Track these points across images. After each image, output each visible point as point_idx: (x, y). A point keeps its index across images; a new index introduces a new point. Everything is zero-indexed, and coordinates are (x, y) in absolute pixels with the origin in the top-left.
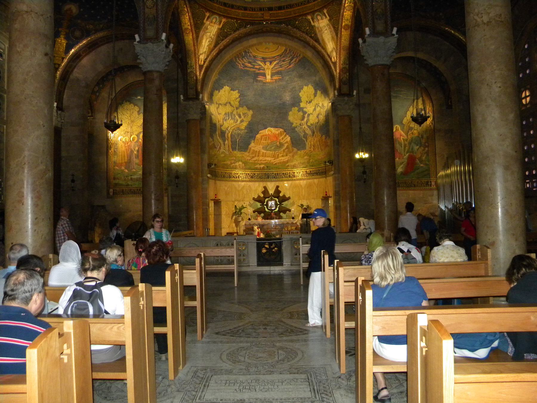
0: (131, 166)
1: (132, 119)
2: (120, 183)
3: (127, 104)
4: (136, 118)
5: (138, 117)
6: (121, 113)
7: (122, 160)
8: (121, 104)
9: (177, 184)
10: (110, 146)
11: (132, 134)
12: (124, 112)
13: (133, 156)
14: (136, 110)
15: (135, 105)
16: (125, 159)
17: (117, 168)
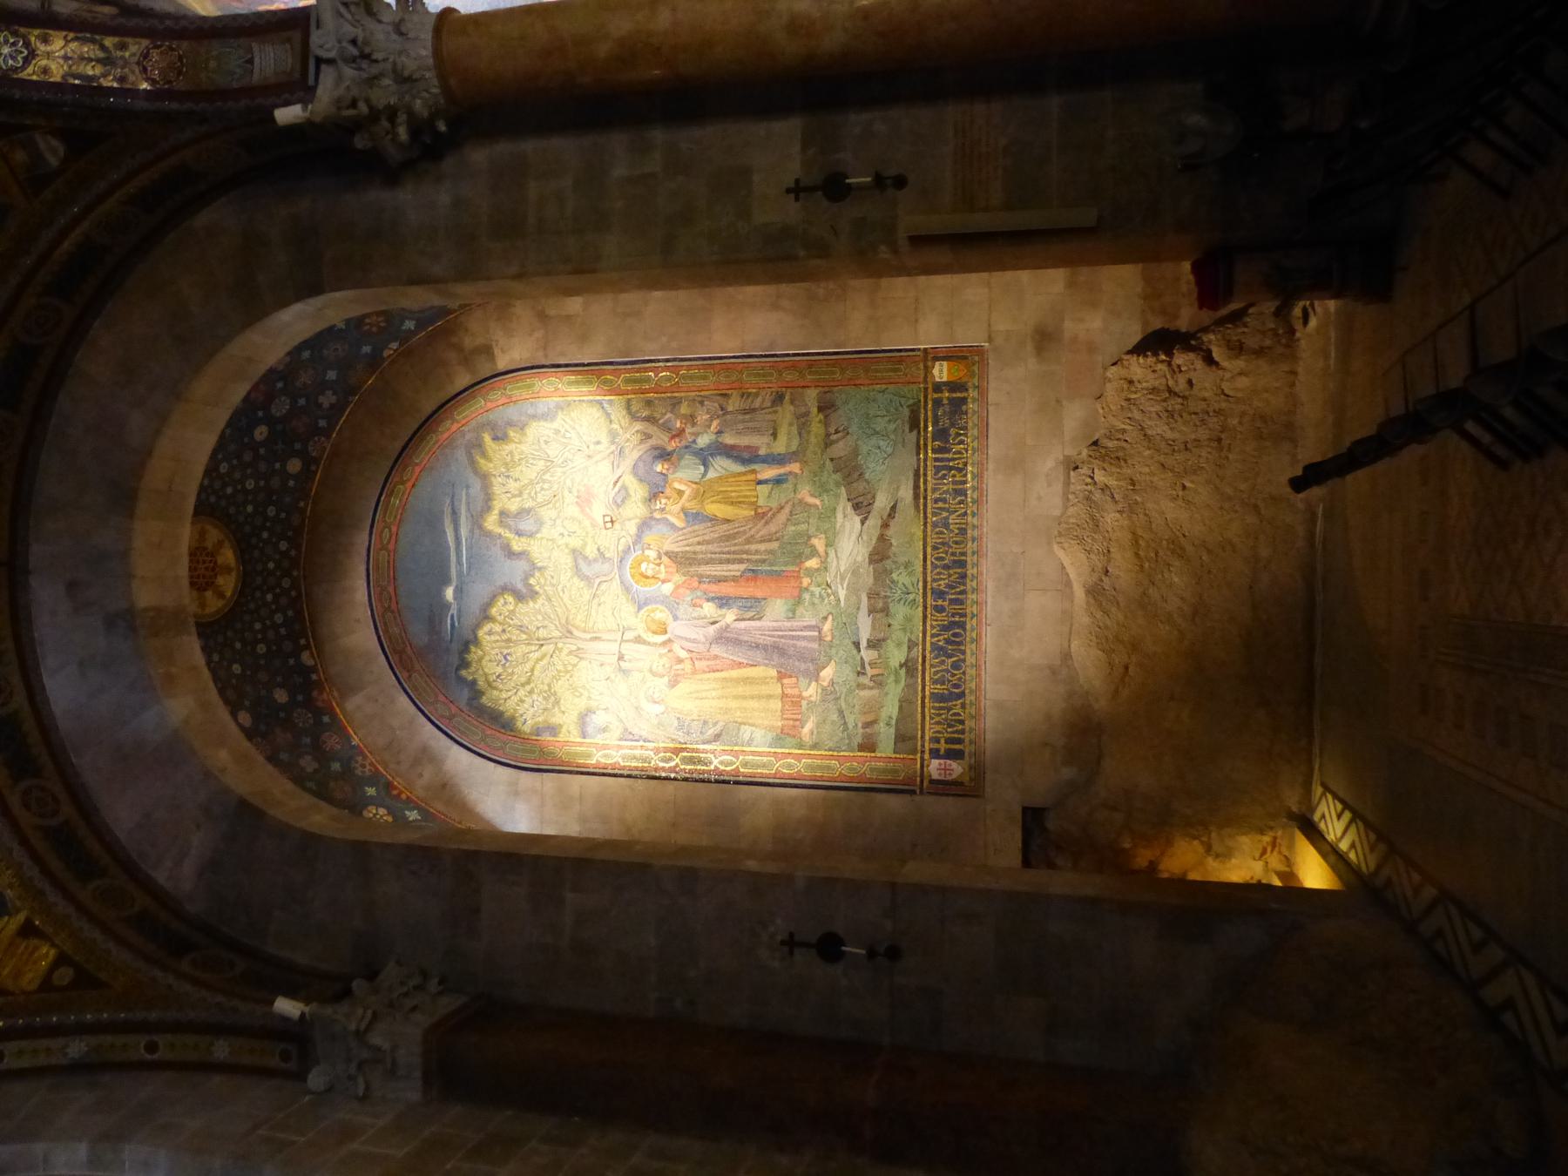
0: (803, 644)
1: (556, 634)
2: (895, 712)
3: (480, 659)
4: (547, 608)
5: (549, 600)
6: (522, 693)
7: (769, 697)
8: (475, 692)
9: (879, 181)
10: (691, 761)
11: (629, 635)
12: (520, 674)
13: (747, 631)
14: (512, 612)
15: (487, 617)
16: (764, 681)
17: (809, 726)
